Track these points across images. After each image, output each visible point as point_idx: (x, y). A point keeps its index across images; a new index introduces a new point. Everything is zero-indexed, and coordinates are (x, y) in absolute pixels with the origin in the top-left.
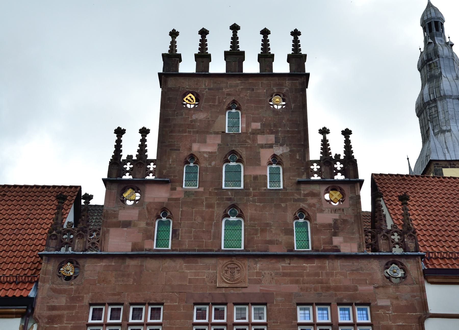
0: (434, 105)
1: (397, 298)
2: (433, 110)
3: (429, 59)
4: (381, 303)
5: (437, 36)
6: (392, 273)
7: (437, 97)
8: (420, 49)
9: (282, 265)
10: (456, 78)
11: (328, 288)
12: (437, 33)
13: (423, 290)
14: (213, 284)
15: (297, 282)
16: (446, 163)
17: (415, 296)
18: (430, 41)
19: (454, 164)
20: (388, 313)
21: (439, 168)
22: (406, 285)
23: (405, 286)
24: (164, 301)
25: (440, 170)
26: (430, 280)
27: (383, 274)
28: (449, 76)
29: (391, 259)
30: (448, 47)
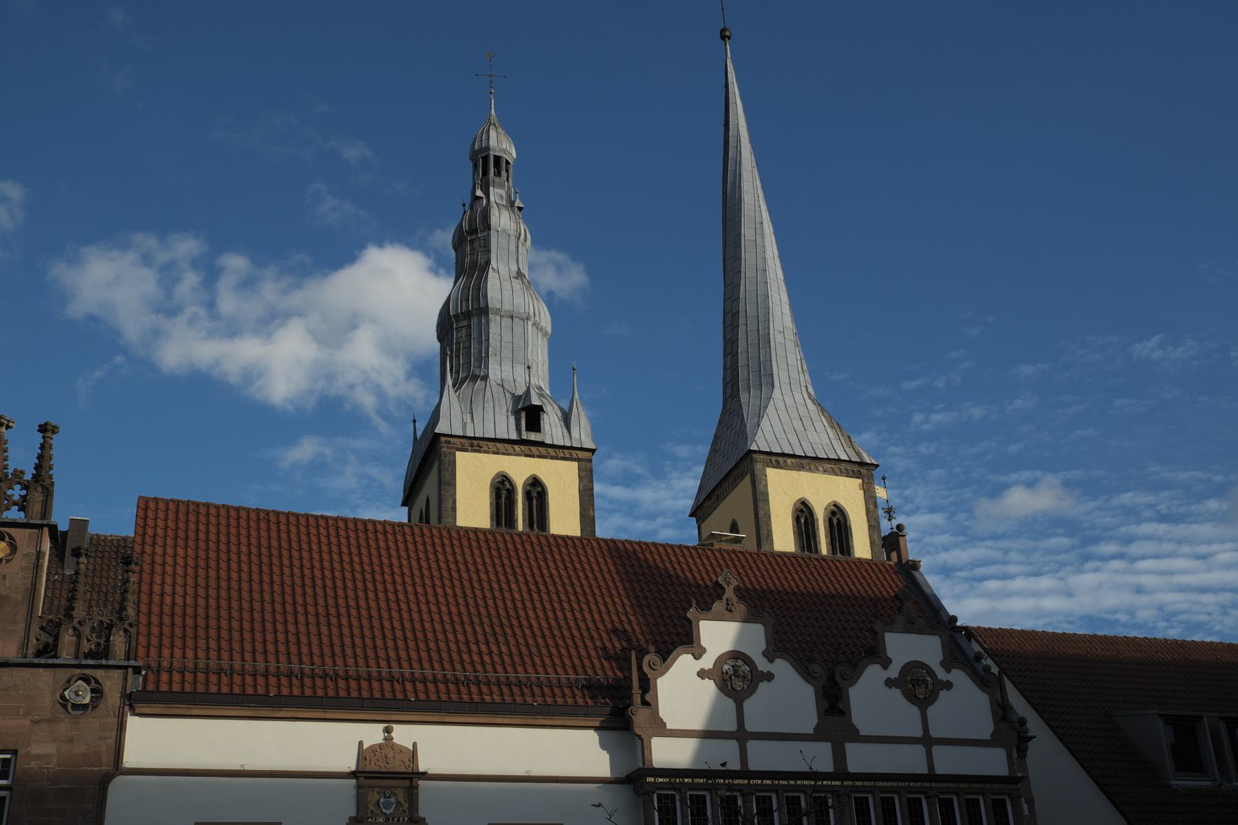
0: (465, 323)
1: (71, 741)
2: (464, 332)
3: (473, 231)
4: (36, 749)
5: (495, 184)
6: (73, 696)
7: (472, 309)
8: (464, 205)
10: (515, 275)
12: (497, 179)
16: (463, 441)
17: (105, 739)
18: (479, 193)
19: (479, 446)
20: (48, 768)
21: (449, 451)
22: (93, 717)
23: (91, 720)
25: (450, 454)
26: (138, 710)
27: (54, 698)
28: (504, 271)
29: (77, 671)
30: (510, 212)
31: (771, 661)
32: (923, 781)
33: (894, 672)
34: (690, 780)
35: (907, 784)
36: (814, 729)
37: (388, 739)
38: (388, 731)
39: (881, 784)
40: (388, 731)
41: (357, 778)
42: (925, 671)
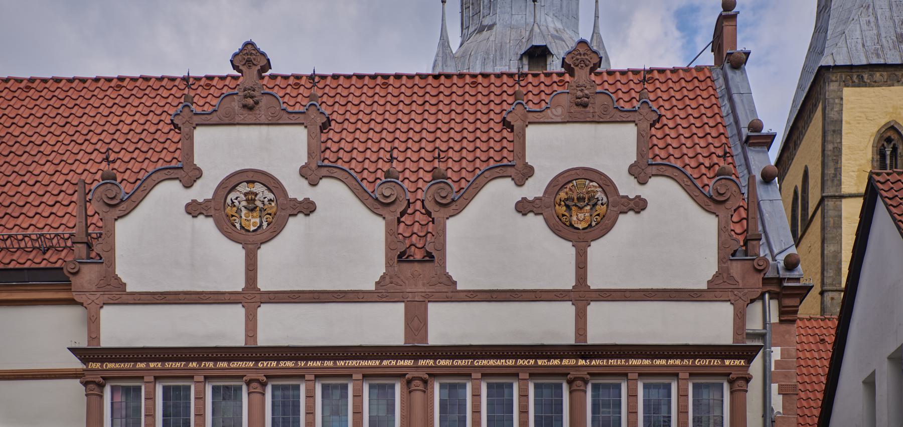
31: (314, 184)
32: (561, 358)
33: (534, 189)
34: (160, 364)
35: (532, 362)
36: (377, 283)
39: (485, 362)
42: (594, 184)
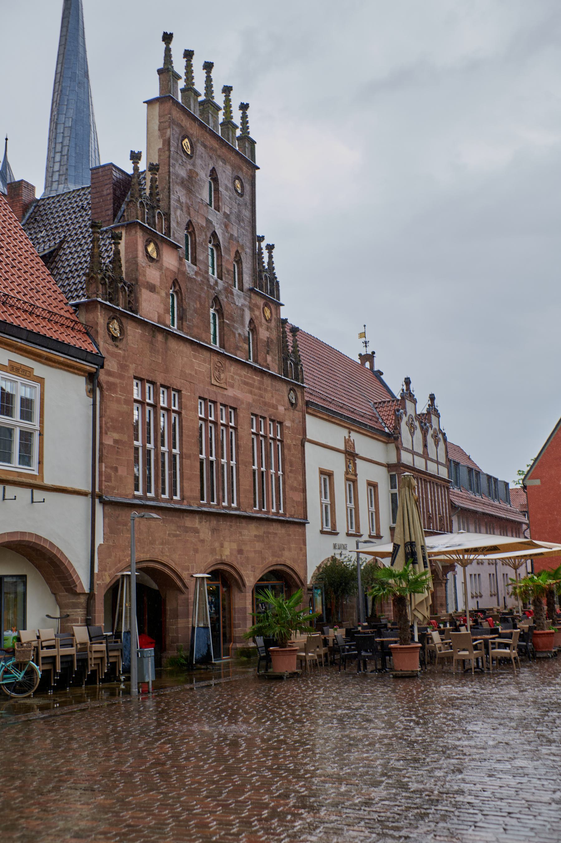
9: (244, 372)
11: (265, 404)
13: (304, 419)
14: (209, 380)
15: (251, 392)
24: (182, 389)
37: (350, 437)
38: (350, 433)
40: (350, 433)
41: (345, 454)
